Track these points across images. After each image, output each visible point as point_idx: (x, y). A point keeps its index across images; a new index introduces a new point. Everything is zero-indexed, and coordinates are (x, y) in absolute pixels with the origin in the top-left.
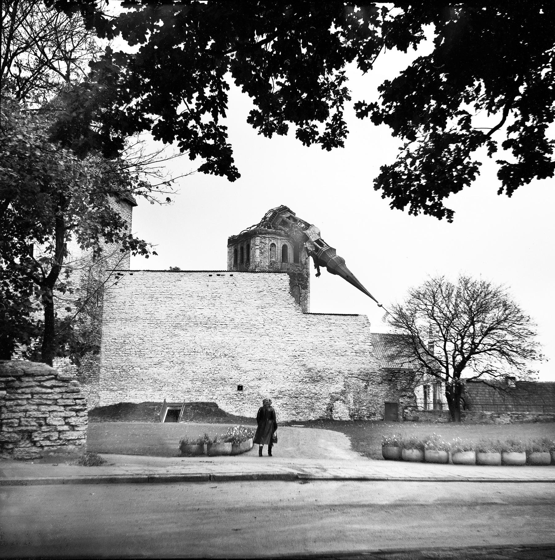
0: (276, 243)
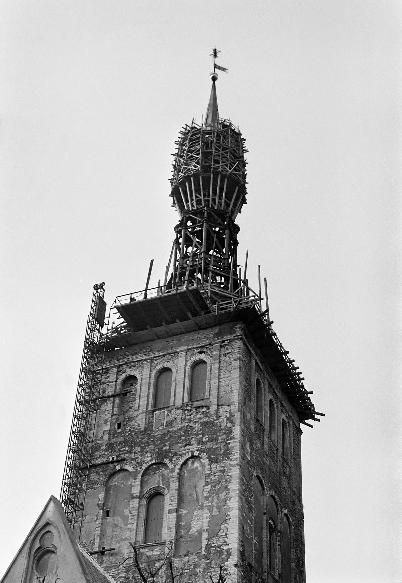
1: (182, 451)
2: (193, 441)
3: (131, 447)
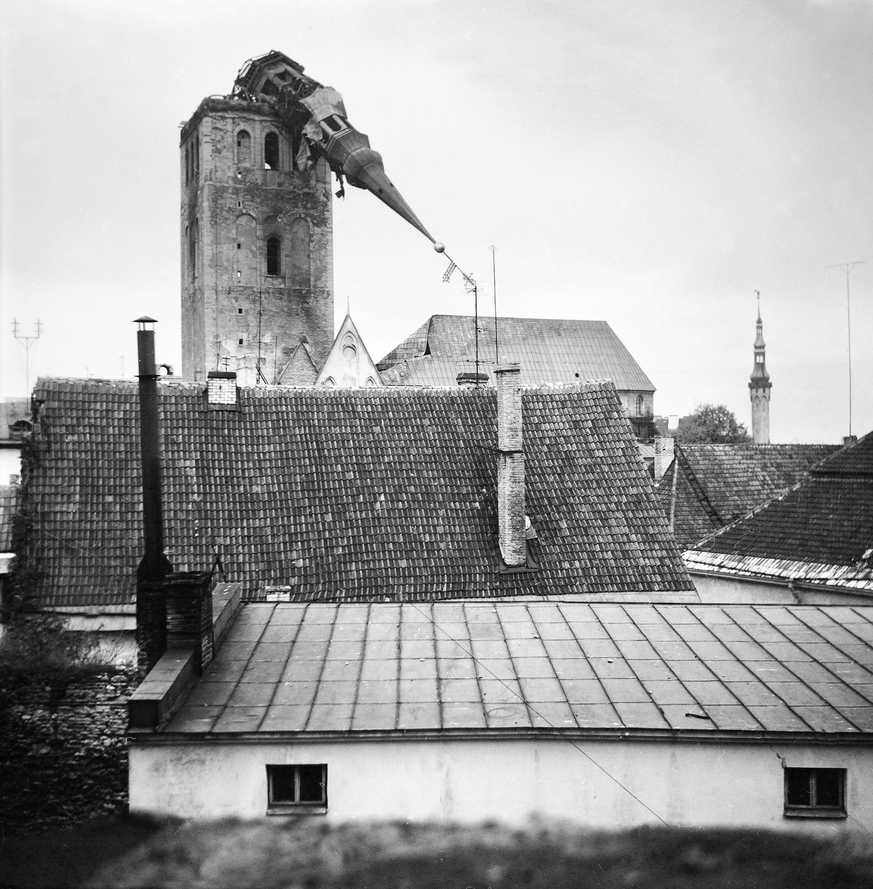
0: (249, 130)
2: (300, 205)
3: (253, 197)
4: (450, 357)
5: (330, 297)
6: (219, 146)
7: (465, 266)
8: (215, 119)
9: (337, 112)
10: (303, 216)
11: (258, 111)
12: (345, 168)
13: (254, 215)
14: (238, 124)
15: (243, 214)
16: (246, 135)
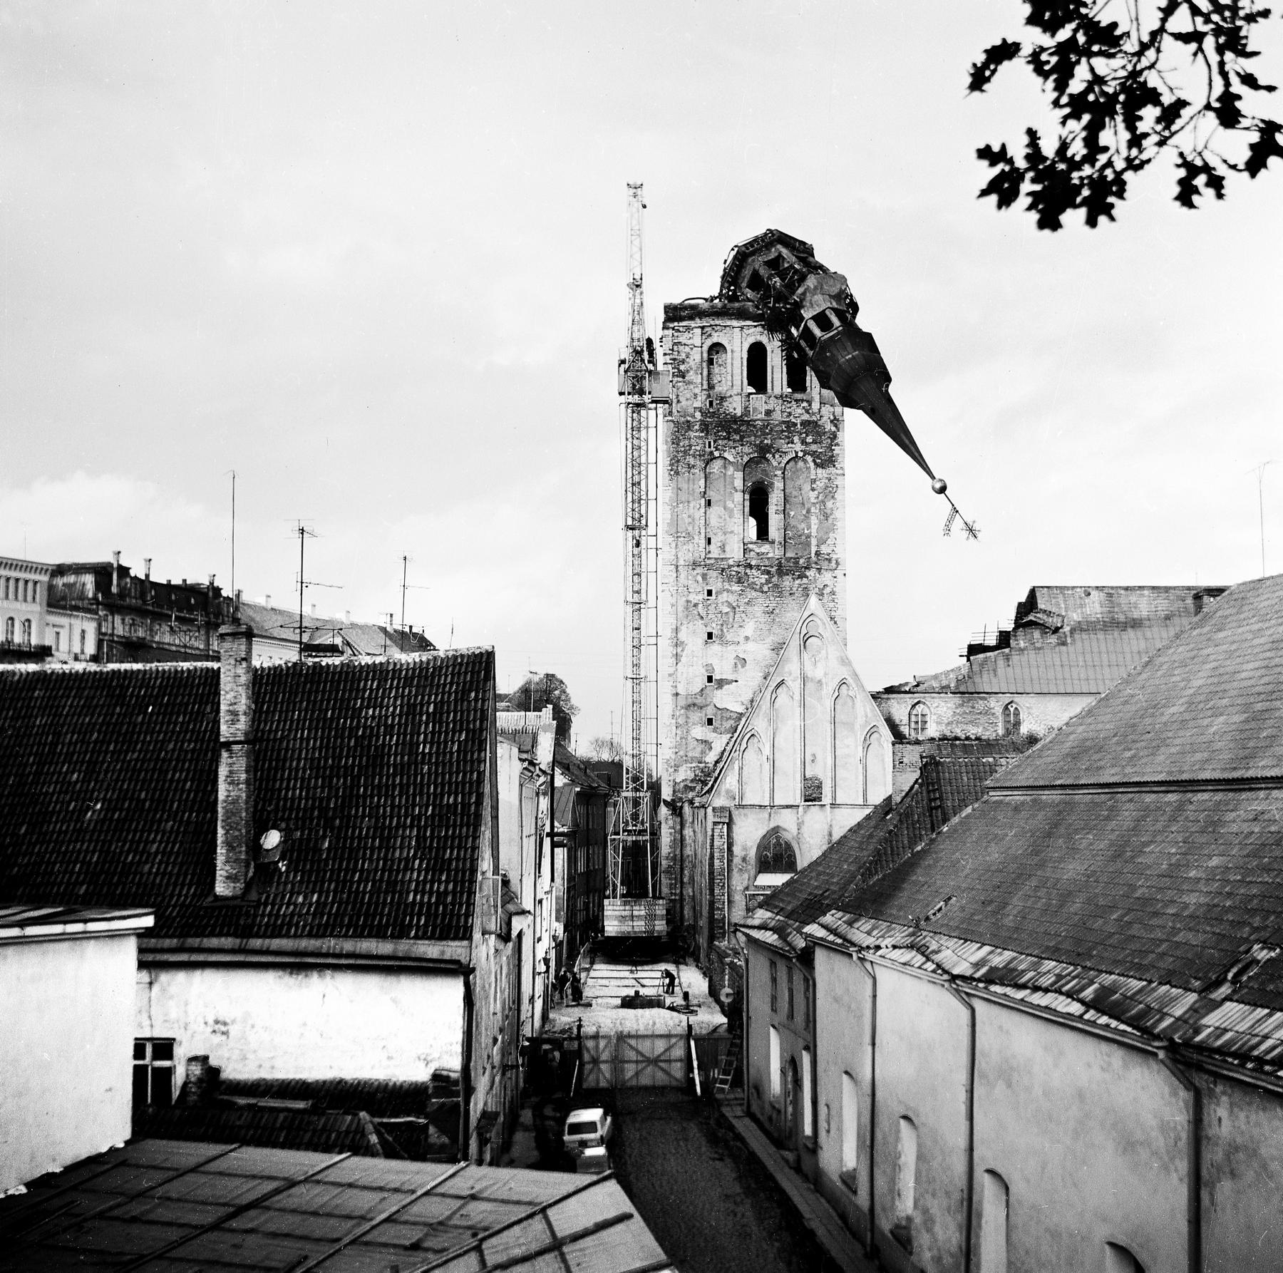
1: (785, 448)
2: (796, 439)
3: (729, 433)
4: (1039, 649)
5: (840, 567)
6: (682, 368)
7: (968, 513)
8: (678, 331)
9: (835, 305)
10: (800, 454)
11: (742, 315)
12: (831, 383)
13: (731, 458)
14: (710, 335)
15: (715, 458)
16: (718, 348)
